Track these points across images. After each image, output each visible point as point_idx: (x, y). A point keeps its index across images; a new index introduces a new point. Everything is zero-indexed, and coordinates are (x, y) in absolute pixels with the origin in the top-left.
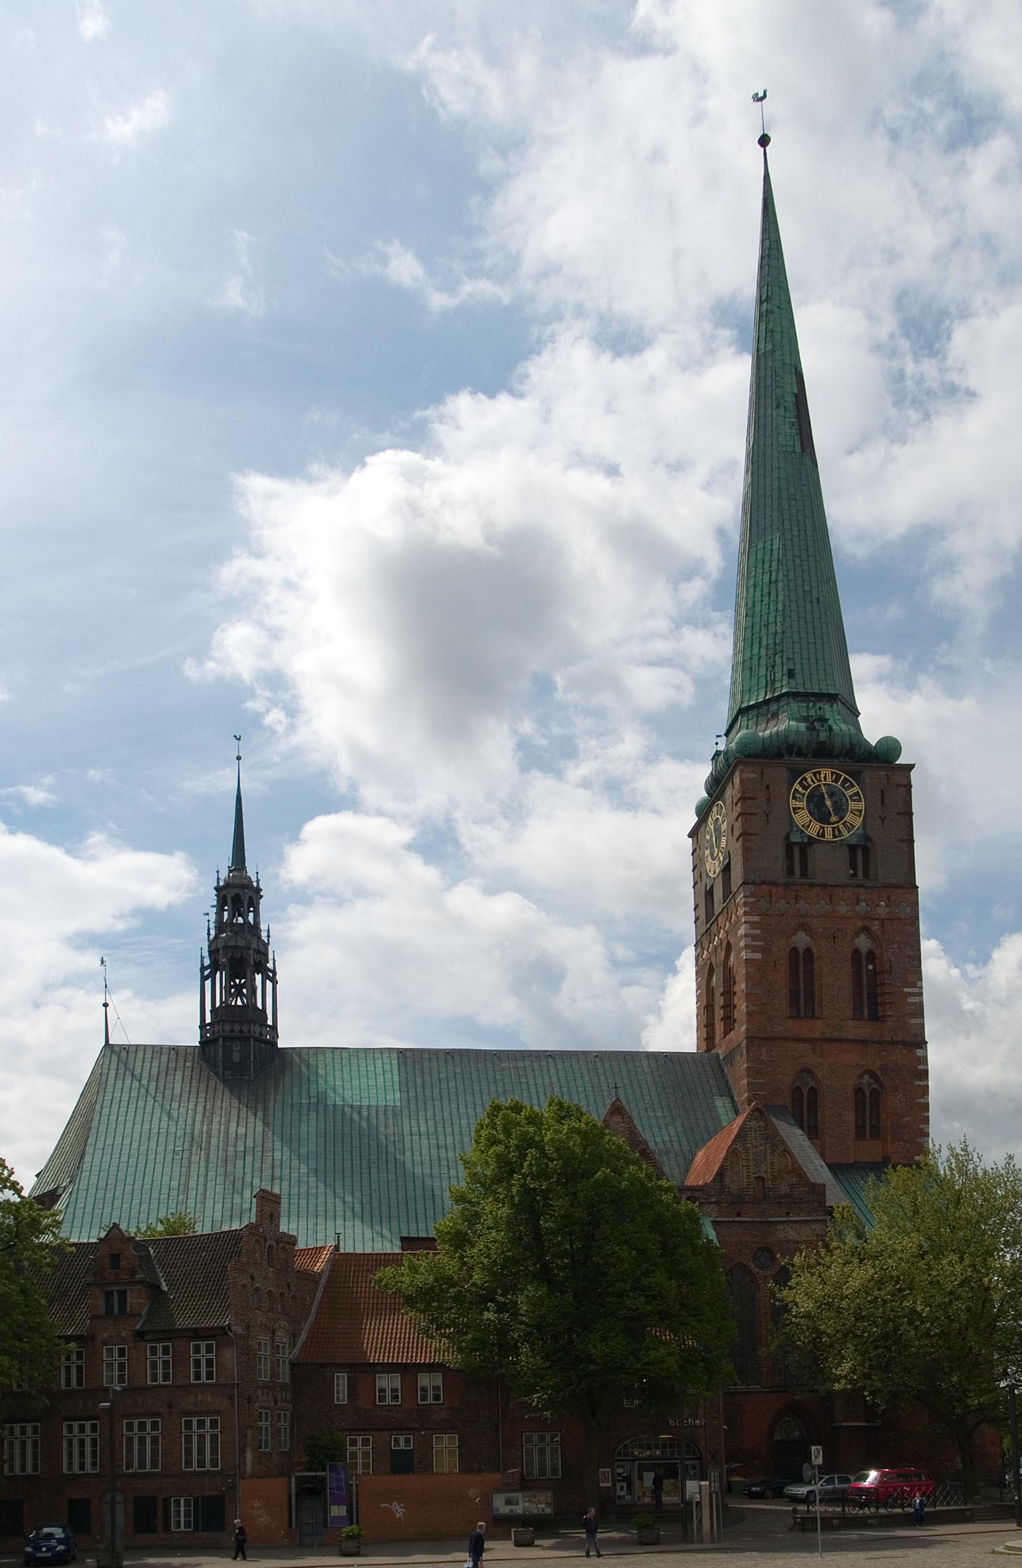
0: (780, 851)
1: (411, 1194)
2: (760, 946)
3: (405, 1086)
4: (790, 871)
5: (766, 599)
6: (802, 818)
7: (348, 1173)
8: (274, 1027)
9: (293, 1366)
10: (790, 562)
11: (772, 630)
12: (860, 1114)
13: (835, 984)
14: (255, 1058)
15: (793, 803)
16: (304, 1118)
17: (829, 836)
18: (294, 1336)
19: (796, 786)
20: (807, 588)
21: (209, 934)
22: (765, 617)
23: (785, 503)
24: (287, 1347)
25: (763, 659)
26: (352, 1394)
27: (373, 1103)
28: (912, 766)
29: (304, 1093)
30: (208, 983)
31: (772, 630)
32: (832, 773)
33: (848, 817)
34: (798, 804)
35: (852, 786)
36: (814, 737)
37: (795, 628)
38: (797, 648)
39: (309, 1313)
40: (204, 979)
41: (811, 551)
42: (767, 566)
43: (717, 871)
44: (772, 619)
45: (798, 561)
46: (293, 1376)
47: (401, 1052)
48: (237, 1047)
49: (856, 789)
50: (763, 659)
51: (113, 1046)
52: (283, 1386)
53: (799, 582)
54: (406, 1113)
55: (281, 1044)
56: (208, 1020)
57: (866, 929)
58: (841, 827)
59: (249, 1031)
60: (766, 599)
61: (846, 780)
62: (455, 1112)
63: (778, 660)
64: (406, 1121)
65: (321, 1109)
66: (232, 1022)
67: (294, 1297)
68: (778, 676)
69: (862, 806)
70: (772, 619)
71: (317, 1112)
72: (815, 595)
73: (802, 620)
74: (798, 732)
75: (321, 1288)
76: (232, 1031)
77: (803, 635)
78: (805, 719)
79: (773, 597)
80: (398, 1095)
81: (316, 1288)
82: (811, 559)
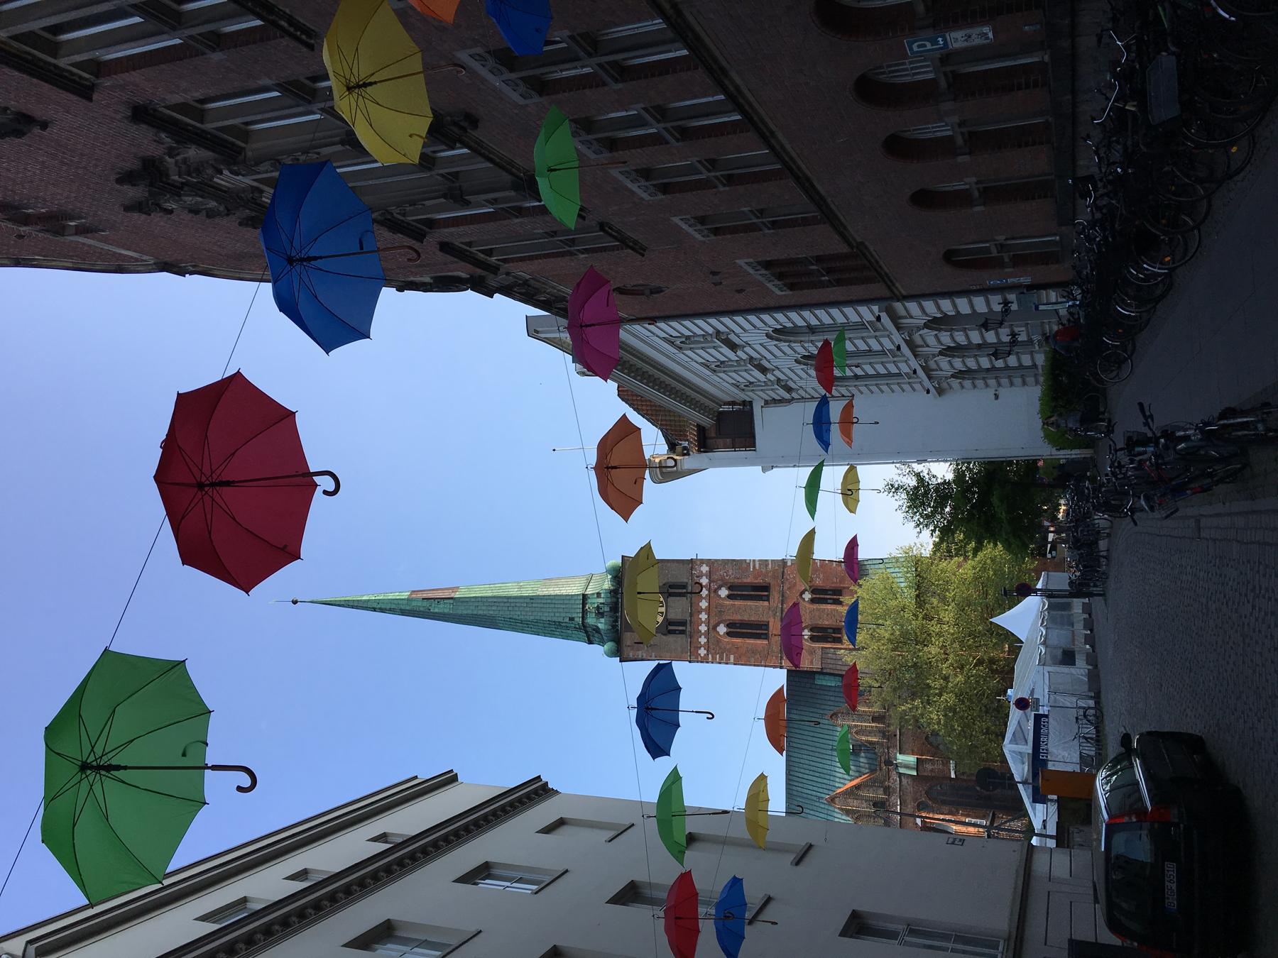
0: (671, 638)
12: (824, 601)
13: (751, 610)
17: (663, 610)
57: (716, 591)
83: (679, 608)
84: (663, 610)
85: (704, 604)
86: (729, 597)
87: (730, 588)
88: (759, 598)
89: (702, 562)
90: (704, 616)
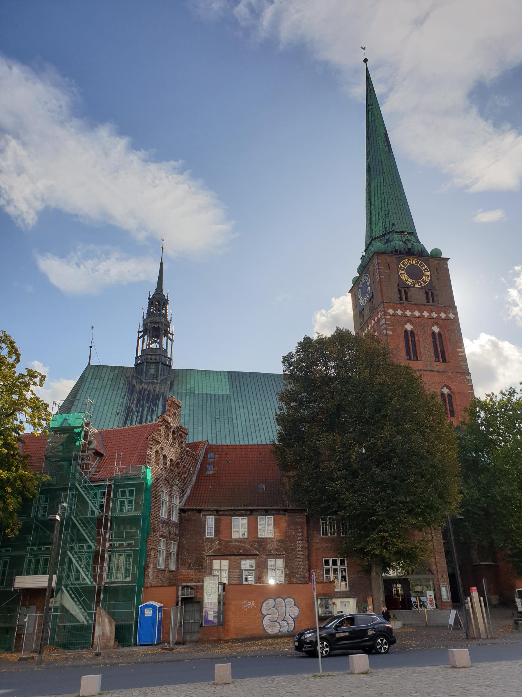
1: (236, 434)
2: (391, 329)
3: (232, 386)
4: (401, 299)
5: (380, 199)
6: (404, 277)
7: (205, 423)
8: (171, 359)
9: (182, 511)
10: (389, 187)
11: (383, 209)
14: (161, 372)
15: (400, 271)
16: (184, 398)
18: (183, 492)
19: (401, 265)
20: (396, 195)
22: (380, 205)
23: (384, 167)
24: (178, 498)
26: (217, 531)
29: (184, 388)
30: (141, 340)
31: (383, 209)
33: (424, 278)
34: (403, 272)
37: (393, 209)
38: (394, 215)
39: (192, 479)
41: (396, 183)
43: (366, 302)
44: (383, 206)
45: (391, 186)
46: (180, 518)
47: (229, 373)
48: (153, 366)
49: (426, 267)
51: (92, 365)
52: (175, 524)
53: (393, 193)
54: (232, 397)
55: (173, 368)
56: (139, 354)
60: (380, 199)
61: (421, 264)
62: (255, 398)
63: (387, 220)
64: (232, 400)
65: (192, 395)
66: (151, 355)
67: (184, 466)
68: (388, 226)
69: (429, 273)
70: (383, 206)
71: (190, 395)
72: (399, 197)
73: (396, 206)
74: (399, 245)
76: (151, 359)
77: (396, 211)
78: (402, 241)
79: (383, 198)
80: (228, 390)
81: (197, 463)
83: (420, 297)
84: (416, 285)
85: (426, 314)
86: (433, 333)
87: (439, 334)
88: (437, 356)
89: (456, 314)
90: (417, 314)
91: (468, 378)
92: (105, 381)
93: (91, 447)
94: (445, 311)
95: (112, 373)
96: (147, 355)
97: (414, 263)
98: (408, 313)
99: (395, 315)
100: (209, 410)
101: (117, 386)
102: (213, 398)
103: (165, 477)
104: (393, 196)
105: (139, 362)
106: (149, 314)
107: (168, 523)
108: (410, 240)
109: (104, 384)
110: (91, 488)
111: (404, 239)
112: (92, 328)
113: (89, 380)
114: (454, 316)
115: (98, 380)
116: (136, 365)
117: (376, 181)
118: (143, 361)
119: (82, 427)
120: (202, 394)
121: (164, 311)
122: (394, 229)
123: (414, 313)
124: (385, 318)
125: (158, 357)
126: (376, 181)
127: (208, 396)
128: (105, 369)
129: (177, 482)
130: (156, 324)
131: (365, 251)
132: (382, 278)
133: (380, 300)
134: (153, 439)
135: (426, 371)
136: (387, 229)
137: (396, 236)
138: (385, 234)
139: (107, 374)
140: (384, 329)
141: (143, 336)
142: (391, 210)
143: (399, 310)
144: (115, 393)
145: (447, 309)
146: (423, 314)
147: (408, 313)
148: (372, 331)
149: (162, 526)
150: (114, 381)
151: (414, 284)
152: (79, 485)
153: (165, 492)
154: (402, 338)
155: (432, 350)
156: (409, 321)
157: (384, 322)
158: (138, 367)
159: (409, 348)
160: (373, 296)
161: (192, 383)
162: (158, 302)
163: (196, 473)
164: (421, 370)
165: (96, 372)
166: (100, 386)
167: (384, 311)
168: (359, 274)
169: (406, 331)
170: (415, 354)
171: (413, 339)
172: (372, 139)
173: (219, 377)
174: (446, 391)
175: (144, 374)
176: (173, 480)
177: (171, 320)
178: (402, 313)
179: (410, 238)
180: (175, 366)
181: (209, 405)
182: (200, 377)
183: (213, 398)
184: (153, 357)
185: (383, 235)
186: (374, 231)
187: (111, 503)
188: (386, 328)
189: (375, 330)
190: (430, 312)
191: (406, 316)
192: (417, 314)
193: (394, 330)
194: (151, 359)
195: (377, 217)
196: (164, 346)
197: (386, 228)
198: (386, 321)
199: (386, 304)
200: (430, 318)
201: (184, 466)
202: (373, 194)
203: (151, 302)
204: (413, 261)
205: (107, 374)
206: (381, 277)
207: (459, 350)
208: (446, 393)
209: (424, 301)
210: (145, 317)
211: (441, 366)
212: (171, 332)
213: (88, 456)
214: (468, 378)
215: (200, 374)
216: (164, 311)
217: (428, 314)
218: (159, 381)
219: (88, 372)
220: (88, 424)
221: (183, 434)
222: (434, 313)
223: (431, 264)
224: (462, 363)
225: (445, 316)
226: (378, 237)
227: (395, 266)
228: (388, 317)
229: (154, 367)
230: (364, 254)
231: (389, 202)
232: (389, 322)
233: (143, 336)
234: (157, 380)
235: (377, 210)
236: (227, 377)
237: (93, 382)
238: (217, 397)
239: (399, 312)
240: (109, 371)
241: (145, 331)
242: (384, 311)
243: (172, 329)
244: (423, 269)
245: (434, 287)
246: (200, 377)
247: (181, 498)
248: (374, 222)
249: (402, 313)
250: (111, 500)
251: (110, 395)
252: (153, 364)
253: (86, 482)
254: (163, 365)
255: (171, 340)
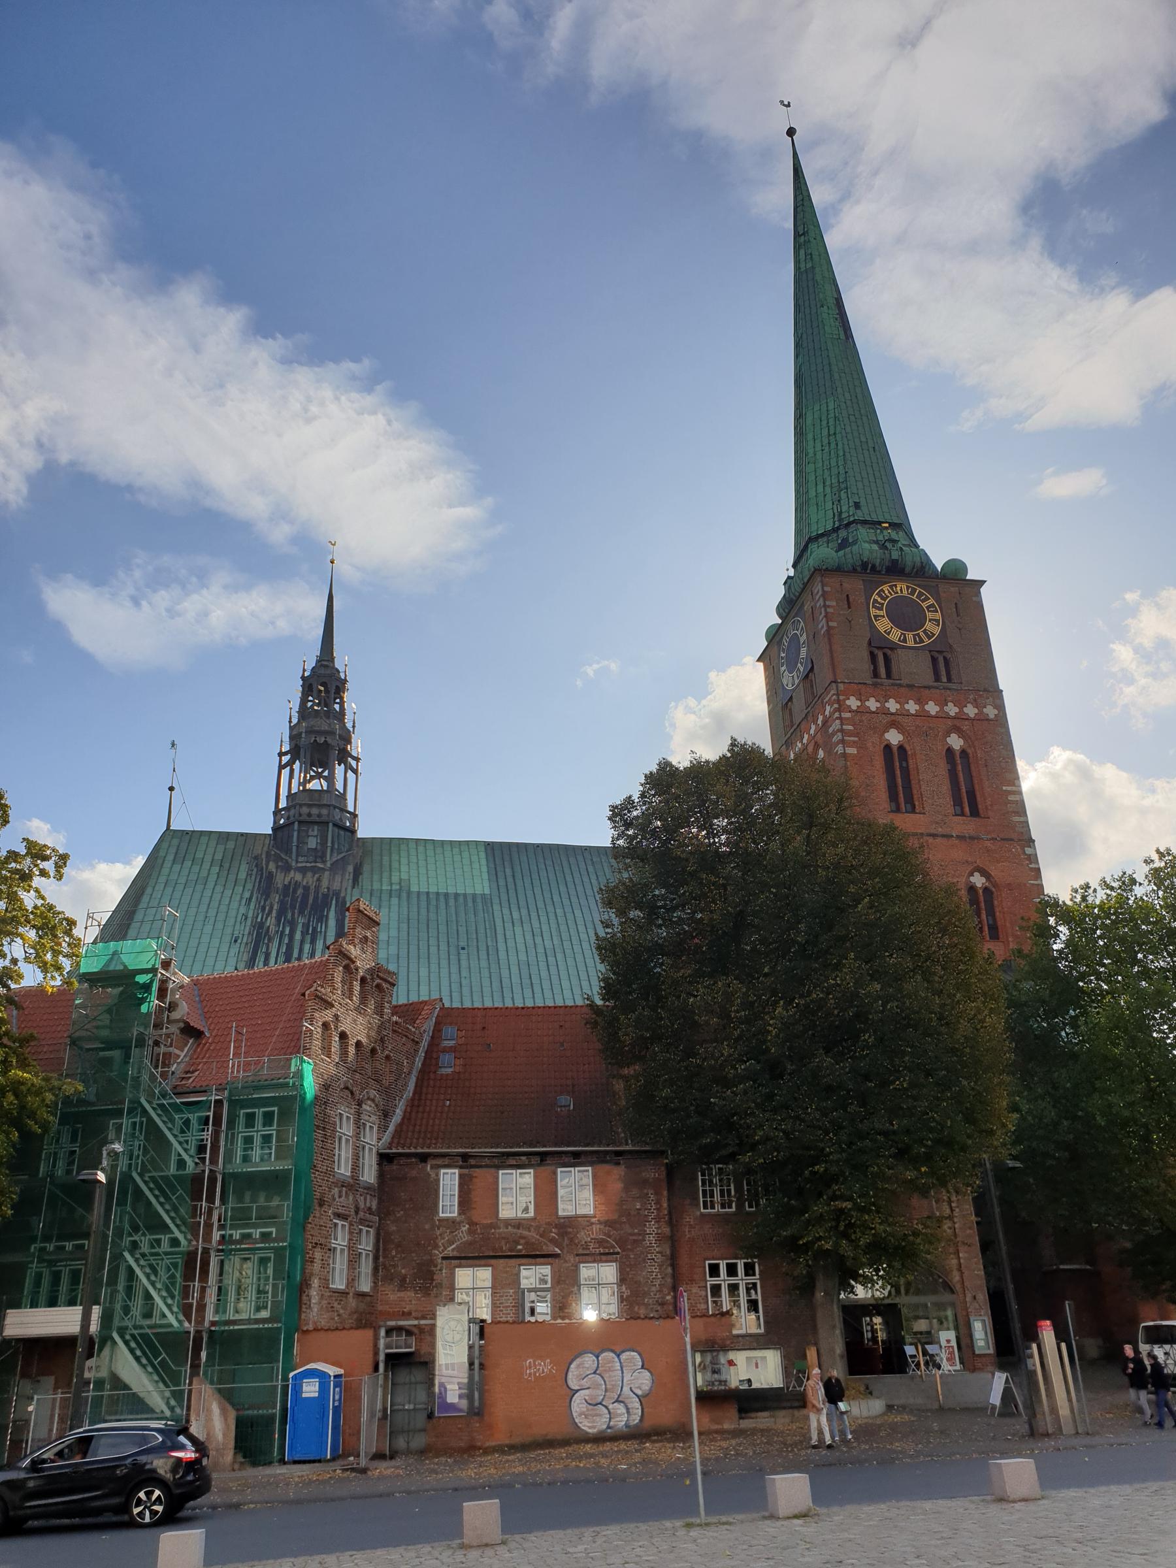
1: (506, 981)
2: (854, 742)
3: (494, 874)
4: (876, 674)
5: (827, 449)
6: (883, 625)
7: (434, 960)
8: (354, 816)
9: (385, 1158)
10: (846, 420)
11: (834, 471)
14: (333, 843)
16: (385, 903)
18: (386, 1115)
19: (875, 596)
20: (863, 439)
21: (290, 722)
23: (836, 376)
24: (375, 1128)
25: (828, 497)
27: (460, 891)
28: (983, 582)
29: (385, 880)
30: (285, 772)
31: (834, 471)
32: (908, 587)
33: (928, 626)
35: (927, 599)
36: (888, 556)
38: (860, 485)
39: (406, 1085)
40: (281, 767)
41: (863, 411)
42: (824, 423)
43: (797, 682)
44: (833, 463)
45: (852, 418)
46: (381, 1175)
48: (315, 831)
49: (931, 601)
50: (828, 497)
53: (856, 434)
54: (496, 901)
55: (360, 835)
56: (283, 804)
58: (922, 634)
59: (328, 815)
60: (827, 449)
62: (548, 901)
64: (496, 907)
65: (404, 895)
66: (310, 806)
67: (388, 1057)
68: (845, 508)
69: (938, 616)
70: (833, 463)
71: (399, 897)
74: (871, 551)
75: (421, 1054)
76: (309, 815)
78: (877, 542)
79: (833, 445)
80: (486, 884)
81: (416, 1051)
82: (864, 418)
85: (932, 708)
86: (950, 751)
87: (963, 752)
88: (957, 801)
89: (1001, 707)
90: (912, 707)
91: (1028, 851)
92: (206, 865)
93: (176, 1015)
94: (975, 700)
95: (221, 848)
96: (301, 805)
97: (905, 593)
98: (892, 705)
99: (862, 711)
100: (443, 928)
101: (232, 877)
102: (452, 902)
103: (346, 1082)
104: (857, 440)
105: (282, 821)
106: (304, 712)
107: (352, 1185)
108: (894, 541)
109: (204, 873)
110: (177, 1108)
111: (881, 538)
112: (173, 745)
113: (168, 864)
114: (996, 712)
115: (188, 863)
116: (276, 829)
117: (817, 407)
118: (292, 819)
119: (153, 970)
120: (428, 893)
121: (337, 707)
122: (859, 515)
123: (907, 706)
124: (840, 718)
125: (324, 811)
126: (817, 407)
127: (442, 899)
128: (204, 840)
129: (373, 1093)
130: (319, 737)
131: (794, 566)
132: (833, 628)
133: (830, 677)
134: (317, 996)
135: (934, 836)
136: (844, 516)
137: (863, 532)
138: (838, 528)
139: (211, 850)
140: (838, 743)
141: (290, 764)
142: (851, 473)
143: (872, 700)
144: (228, 893)
145: (981, 696)
146: (926, 707)
147: (892, 705)
148: (810, 749)
149: (340, 1192)
150: (226, 865)
151: (905, 641)
152: (149, 1102)
153: (345, 1115)
154: (879, 763)
155: (946, 787)
156: (894, 724)
157: (839, 727)
158: (279, 834)
159: (896, 786)
160: (812, 669)
161: (404, 868)
162: (324, 685)
163: (415, 1073)
164: (922, 834)
165: (184, 846)
166: (193, 877)
167: (838, 701)
168: (781, 617)
169: (888, 747)
170: (910, 800)
171: (904, 765)
172: (807, 311)
173: (466, 854)
174: (978, 881)
175: (294, 849)
176: (363, 1089)
177: (354, 727)
178: (878, 705)
179: (894, 535)
180: (364, 831)
181: (442, 918)
182: (421, 857)
183: (452, 902)
184: (315, 811)
185: (835, 530)
186: (814, 519)
187: (222, 1143)
188: (842, 741)
189: (817, 746)
190: (942, 703)
191: (887, 713)
192: (912, 707)
193: (861, 746)
194: (309, 815)
195: (820, 488)
196: (339, 786)
197: (840, 513)
198: (842, 724)
199: (841, 686)
200: (942, 716)
201: (388, 1057)
202: (810, 436)
203: (308, 686)
204: (902, 588)
205: (211, 850)
206: (831, 624)
207: (1009, 788)
208: (979, 885)
209: (929, 679)
210: (295, 721)
211: (964, 825)
212: (354, 754)
213: (168, 1036)
214: (1028, 851)
215: (421, 849)
216: (337, 707)
217: (938, 709)
218: (328, 864)
219: (165, 845)
220: (166, 964)
221: (385, 985)
222: (950, 704)
223: (942, 594)
224: (1016, 819)
225: (976, 711)
226: (822, 535)
227: (863, 600)
228: (848, 715)
229: (315, 833)
230: (792, 573)
231: (848, 455)
232: (851, 727)
233: (290, 764)
234: (324, 862)
235: (819, 472)
236: (483, 855)
237: (177, 867)
238: (461, 899)
239: (872, 704)
240: (213, 843)
241: (295, 752)
242: (838, 701)
243: (357, 747)
244: (924, 605)
245: (951, 647)
246: (421, 857)
247: (383, 1128)
248: (813, 501)
249: (878, 705)
250: (223, 1136)
251: (217, 896)
252: (314, 829)
253: (164, 1095)
254: (336, 830)
255: (355, 771)
